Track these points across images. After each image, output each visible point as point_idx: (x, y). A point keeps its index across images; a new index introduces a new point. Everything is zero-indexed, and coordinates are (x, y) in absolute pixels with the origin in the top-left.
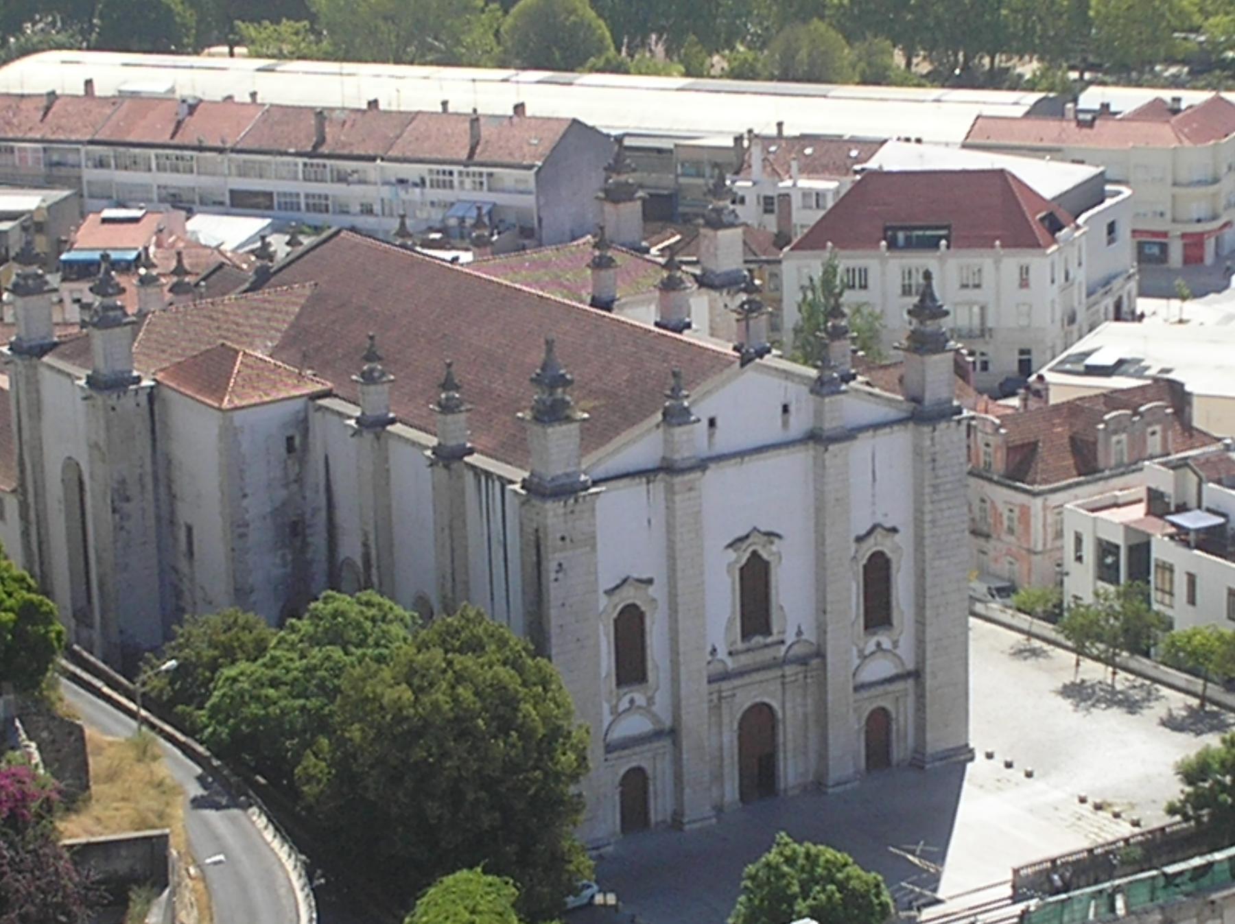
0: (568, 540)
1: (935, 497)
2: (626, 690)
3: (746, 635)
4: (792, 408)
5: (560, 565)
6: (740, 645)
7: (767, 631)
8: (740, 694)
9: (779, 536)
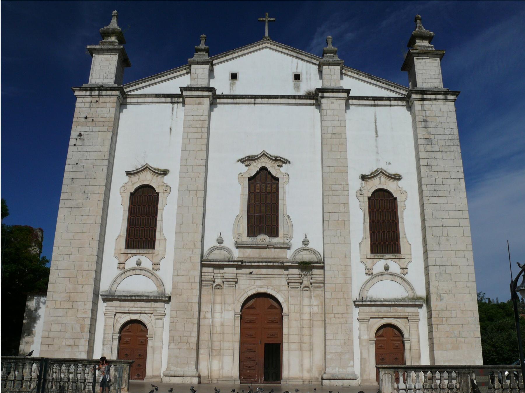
0: (90, 120)
1: (429, 148)
2: (134, 251)
3: (252, 232)
4: (303, 77)
5: (80, 135)
6: (245, 239)
7: (274, 232)
8: (243, 283)
9: (287, 162)
